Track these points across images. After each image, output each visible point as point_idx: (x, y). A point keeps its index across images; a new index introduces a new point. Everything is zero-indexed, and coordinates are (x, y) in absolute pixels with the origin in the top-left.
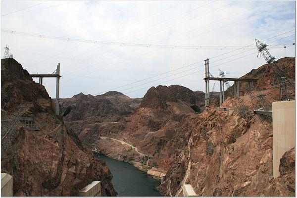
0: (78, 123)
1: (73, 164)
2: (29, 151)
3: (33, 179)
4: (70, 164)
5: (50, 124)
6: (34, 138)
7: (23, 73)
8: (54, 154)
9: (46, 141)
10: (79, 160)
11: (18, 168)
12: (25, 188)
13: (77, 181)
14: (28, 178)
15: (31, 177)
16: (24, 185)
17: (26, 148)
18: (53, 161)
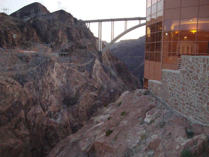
0: (137, 58)
1: (96, 89)
2: (57, 77)
3: (54, 97)
4: (93, 89)
5: (84, 58)
6: (63, 67)
7: (73, 20)
8: (77, 81)
9: (73, 70)
10: (105, 86)
11: (40, 88)
12: (44, 102)
13: (98, 102)
14: (49, 96)
15: (52, 96)
16: (43, 100)
17: (54, 76)
18: (75, 86)
